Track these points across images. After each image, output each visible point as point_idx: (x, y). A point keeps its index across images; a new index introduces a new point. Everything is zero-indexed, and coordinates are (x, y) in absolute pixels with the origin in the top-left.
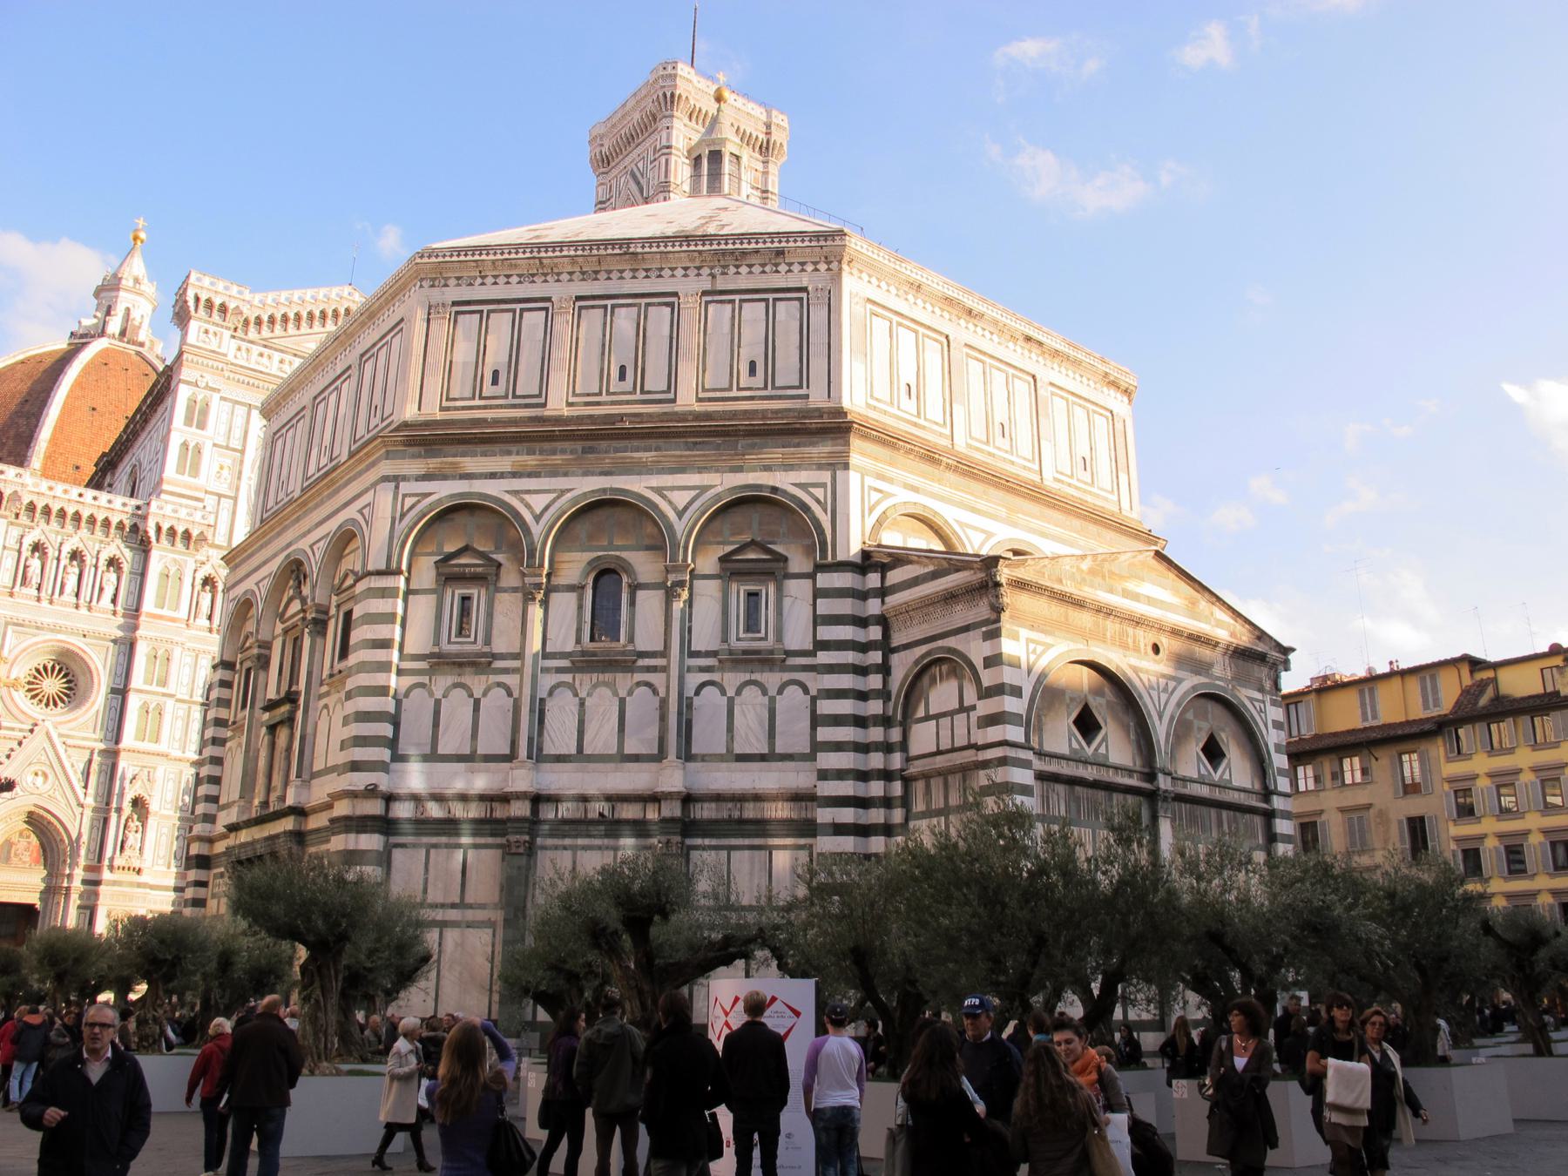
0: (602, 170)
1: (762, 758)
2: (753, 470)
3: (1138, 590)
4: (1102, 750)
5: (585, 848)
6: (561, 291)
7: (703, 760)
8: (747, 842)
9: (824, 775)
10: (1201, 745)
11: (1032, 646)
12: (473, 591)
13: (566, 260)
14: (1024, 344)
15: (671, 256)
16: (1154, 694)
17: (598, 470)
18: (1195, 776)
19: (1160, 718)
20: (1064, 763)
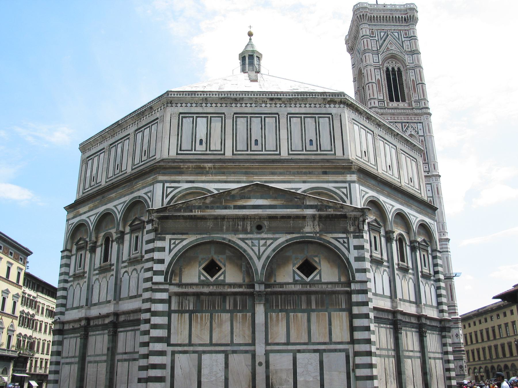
0: (351, 53)
1: (135, 297)
2: (136, 191)
3: (245, 204)
4: (222, 278)
5: (98, 334)
6: (105, 144)
7: (123, 300)
8: (130, 328)
9: (145, 301)
10: (297, 266)
11: (173, 241)
12: (83, 252)
13: (106, 133)
14: (270, 102)
15: (127, 121)
16: (256, 249)
17: (104, 204)
18: (291, 280)
19: (259, 258)
20: (194, 287)
